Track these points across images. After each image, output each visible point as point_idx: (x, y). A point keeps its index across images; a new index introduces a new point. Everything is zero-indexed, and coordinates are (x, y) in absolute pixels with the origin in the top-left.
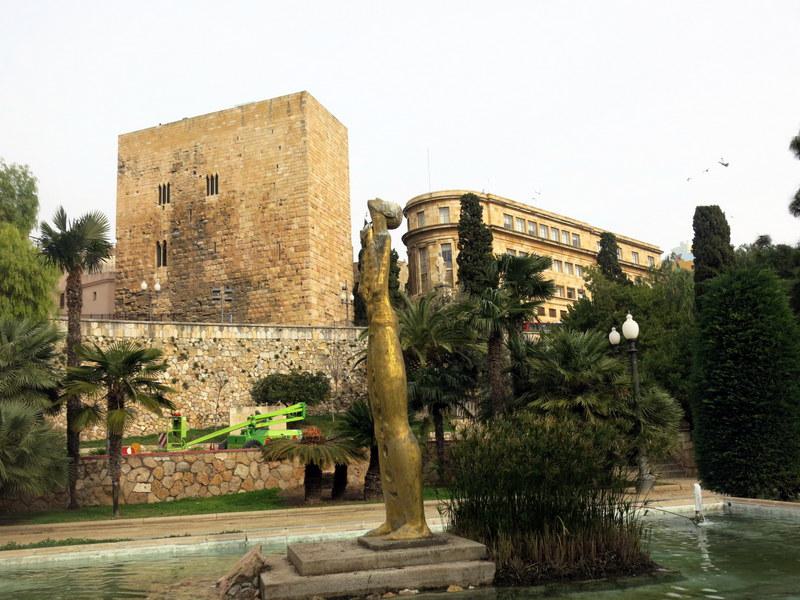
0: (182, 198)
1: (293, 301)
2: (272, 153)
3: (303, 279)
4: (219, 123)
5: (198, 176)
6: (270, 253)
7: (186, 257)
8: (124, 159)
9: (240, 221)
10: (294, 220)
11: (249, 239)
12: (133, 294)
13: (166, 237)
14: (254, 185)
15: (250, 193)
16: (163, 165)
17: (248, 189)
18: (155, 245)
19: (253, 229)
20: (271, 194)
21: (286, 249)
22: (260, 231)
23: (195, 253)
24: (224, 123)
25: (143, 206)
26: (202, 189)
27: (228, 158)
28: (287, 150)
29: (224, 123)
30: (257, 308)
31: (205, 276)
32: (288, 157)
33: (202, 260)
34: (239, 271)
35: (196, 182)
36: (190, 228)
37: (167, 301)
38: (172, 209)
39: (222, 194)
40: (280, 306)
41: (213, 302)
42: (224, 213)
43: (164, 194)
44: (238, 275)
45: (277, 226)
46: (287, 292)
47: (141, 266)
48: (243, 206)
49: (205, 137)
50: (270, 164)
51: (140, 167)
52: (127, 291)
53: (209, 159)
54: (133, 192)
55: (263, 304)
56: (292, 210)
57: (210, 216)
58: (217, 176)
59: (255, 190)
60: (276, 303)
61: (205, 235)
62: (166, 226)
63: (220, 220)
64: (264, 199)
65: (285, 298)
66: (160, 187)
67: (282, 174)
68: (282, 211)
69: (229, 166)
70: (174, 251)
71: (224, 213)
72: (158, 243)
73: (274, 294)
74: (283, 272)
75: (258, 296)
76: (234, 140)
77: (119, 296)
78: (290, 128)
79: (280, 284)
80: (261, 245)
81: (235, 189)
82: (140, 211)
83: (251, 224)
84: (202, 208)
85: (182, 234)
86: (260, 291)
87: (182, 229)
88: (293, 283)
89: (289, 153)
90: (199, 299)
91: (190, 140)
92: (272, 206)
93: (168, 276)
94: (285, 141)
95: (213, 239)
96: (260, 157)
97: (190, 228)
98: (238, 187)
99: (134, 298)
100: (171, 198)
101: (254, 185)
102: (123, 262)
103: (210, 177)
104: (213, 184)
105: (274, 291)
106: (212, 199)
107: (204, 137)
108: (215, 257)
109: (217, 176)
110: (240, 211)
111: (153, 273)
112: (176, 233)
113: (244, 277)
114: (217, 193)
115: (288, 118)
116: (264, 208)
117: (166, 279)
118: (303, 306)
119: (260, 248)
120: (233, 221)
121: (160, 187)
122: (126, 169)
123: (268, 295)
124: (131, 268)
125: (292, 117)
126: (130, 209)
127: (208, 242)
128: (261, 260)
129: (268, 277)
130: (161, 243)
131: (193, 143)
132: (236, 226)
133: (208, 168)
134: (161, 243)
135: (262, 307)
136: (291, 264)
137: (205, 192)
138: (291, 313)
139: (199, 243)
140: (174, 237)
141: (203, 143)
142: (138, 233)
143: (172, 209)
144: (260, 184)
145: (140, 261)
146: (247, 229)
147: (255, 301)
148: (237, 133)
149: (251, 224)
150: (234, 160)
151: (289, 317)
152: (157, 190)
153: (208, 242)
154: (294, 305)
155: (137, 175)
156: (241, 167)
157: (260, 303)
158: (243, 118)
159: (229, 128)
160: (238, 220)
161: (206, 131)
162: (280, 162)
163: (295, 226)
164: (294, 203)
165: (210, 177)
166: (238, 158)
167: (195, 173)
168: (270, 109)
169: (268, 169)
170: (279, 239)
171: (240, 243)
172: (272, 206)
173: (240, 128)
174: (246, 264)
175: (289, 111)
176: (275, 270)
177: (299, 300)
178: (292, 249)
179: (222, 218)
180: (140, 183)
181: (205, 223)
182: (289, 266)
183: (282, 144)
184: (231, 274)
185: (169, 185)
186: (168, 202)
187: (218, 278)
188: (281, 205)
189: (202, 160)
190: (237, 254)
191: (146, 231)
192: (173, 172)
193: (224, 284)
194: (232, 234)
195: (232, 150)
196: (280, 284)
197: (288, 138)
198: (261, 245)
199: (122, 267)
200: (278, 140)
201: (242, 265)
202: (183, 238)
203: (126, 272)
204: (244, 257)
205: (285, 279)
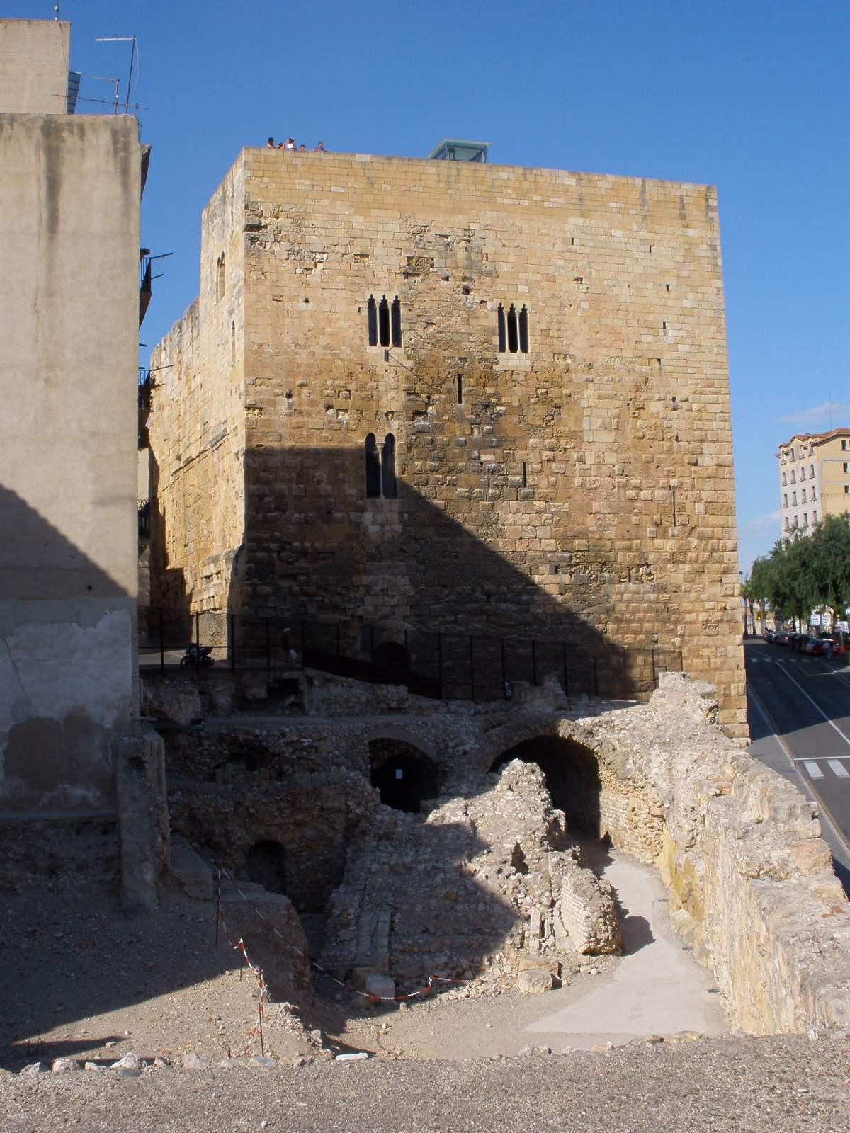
0: (437, 342)
1: (703, 617)
2: (650, 292)
3: (726, 572)
4: (525, 194)
5: (474, 297)
6: (653, 507)
7: (452, 484)
8: (266, 207)
9: (585, 426)
10: (705, 445)
11: (605, 469)
12: (304, 553)
13: (395, 427)
14: (613, 352)
15: (608, 368)
16: (378, 250)
17: (599, 362)
18: (362, 441)
19: (617, 448)
20: (654, 382)
21: (688, 504)
22: (630, 454)
23: (473, 477)
24: (535, 198)
25: (324, 341)
26: (486, 332)
27: (552, 279)
28: (682, 297)
29: (535, 198)
30: (628, 621)
31: (500, 533)
32: (686, 313)
33: (495, 498)
34: (585, 535)
35: (471, 313)
36: (459, 418)
37: (403, 582)
38: (410, 364)
39: (539, 357)
40: (677, 622)
41: (525, 598)
42: (545, 399)
43: (384, 323)
44: (579, 543)
45: (670, 450)
46: (693, 595)
47: (325, 487)
48: (590, 391)
49: (489, 214)
50: (651, 317)
51: (315, 240)
52: (284, 544)
53: (505, 268)
54: (292, 299)
55: (641, 615)
56: (697, 424)
57: (512, 397)
58: (524, 310)
59: (617, 363)
60: (667, 615)
61: (498, 441)
62: (393, 400)
63: (535, 414)
64: (637, 389)
65: (689, 606)
66: (372, 302)
67: (675, 345)
68: (679, 423)
69: (553, 296)
70: (418, 463)
71: (545, 399)
72: (371, 438)
73: (666, 596)
74: (683, 551)
75: (626, 596)
76: (564, 242)
77: (260, 555)
78: (688, 250)
79: (678, 575)
80: (635, 488)
81: (572, 351)
82: (319, 350)
83: (610, 437)
84: (491, 377)
85: (441, 429)
86: (631, 586)
87: (439, 416)
88: (705, 578)
89: (688, 304)
90: (488, 586)
91: (452, 212)
92: (655, 407)
93: (405, 525)
94: (678, 277)
95: (519, 454)
96: (624, 294)
97: (459, 418)
98: (578, 346)
99: (303, 563)
100: (406, 337)
101: (613, 352)
102: (267, 469)
103: (506, 311)
104: (513, 330)
105: (661, 589)
106: (512, 361)
107: (489, 216)
108: (526, 497)
109: (524, 310)
110: (583, 404)
111: (362, 510)
112: (420, 423)
113: (598, 549)
114: (525, 350)
115: (682, 231)
116: (639, 409)
117: (398, 528)
118: (724, 627)
119: (631, 493)
120: (567, 422)
121: (372, 302)
122: (271, 238)
123: (653, 596)
124: (296, 489)
125: (691, 232)
126: (287, 339)
127: (506, 459)
128: (634, 519)
129: (652, 557)
130: (380, 439)
131: (460, 220)
132: (575, 435)
133: (502, 287)
134: (380, 439)
135: (641, 621)
136: (701, 538)
137: (496, 341)
138: (703, 640)
139: (483, 458)
140: (422, 431)
141: (486, 228)
142: (313, 403)
143: (410, 364)
144: (627, 354)
145: (321, 474)
146: (603, 447)
147: (622, 606)
148: (567, 227)
149: (610, 437)
150: (565, 287)
151: (698, 648)
152: (365, 308)
153: (506, 459)
154: (706, 624)
155: (304, 259)
156: (585, 305)
157: (633, 613)
158: (581, 200)
159: (549, 212)
160: (579, 420)
161: (491, 202)
162: (670, 319)
163: (707, 461)
164: (699, 411)
165: (506, 311)
166: (575, 285)
167: (467, 291)
168: (644, 203)
169: (648, 326)
170: (674, 482)
171: (585, 473)
172: (655, 407)
173: (575, 220)
174: (601, 522)
175: (683, 217)
176: (670, 544)
177: (718, 615)
178: (699, 507)
179: (542, 410)
180: (314, 278)
181: (500, 414)
182: (694, 541)
183: (673, 283)
184: (565, 540)
185: (397, 302)
186: (397, 343)
187: (535, 545)
188: (675, 409)
189: (488, 266)
190: (578, 497)
191: (336, 403)
192: (407, 275)
193: (551, 562)
194: (565, 450)
195: (561, 263)
196: (678, 575)
197: (685, 273)
198: (635, 488)
199: (267, 482)
200: (663, 272)
201: (591, 524)
202: (440, 437)
203: (279, 497)
204: (595, 506)
205: (687, 567)
